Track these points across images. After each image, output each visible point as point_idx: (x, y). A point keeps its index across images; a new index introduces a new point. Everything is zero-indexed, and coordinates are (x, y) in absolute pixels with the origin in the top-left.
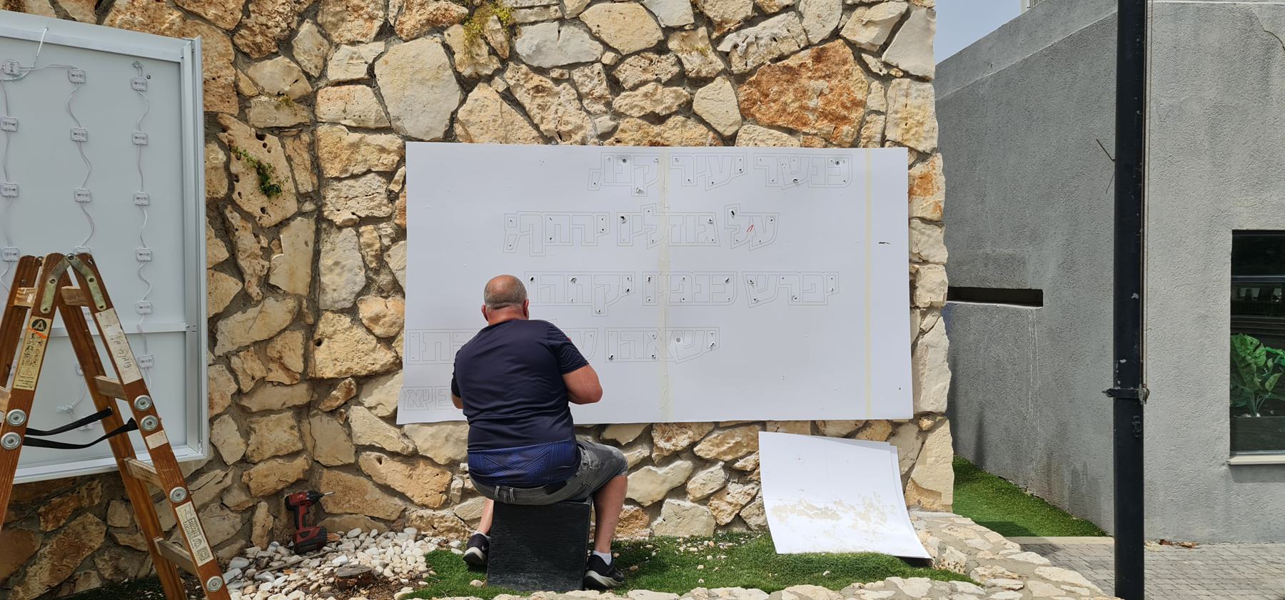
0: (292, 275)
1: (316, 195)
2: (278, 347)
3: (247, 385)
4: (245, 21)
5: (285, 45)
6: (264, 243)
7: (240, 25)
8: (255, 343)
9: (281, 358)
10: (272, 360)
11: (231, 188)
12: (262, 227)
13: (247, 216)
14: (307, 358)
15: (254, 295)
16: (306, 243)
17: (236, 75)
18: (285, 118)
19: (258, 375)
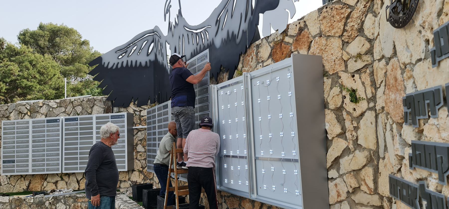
0: (366, 139)
1: (373, 99)
2: (363, 174)
3: (351, 191)
4: (346, 28)
5: (361, 30)
6: (355, 125)
7: (344, 30)
8: (354, 170)
9: (365, 180)
10: (362, 180)
11: (343, 102)
12: (354, 117)
13: (348, 113)
14: (375, 182)
15: (351, 148)
16: (371, 123)
17: (342, 53)
18: (360, 65)
19: (353, 186)
